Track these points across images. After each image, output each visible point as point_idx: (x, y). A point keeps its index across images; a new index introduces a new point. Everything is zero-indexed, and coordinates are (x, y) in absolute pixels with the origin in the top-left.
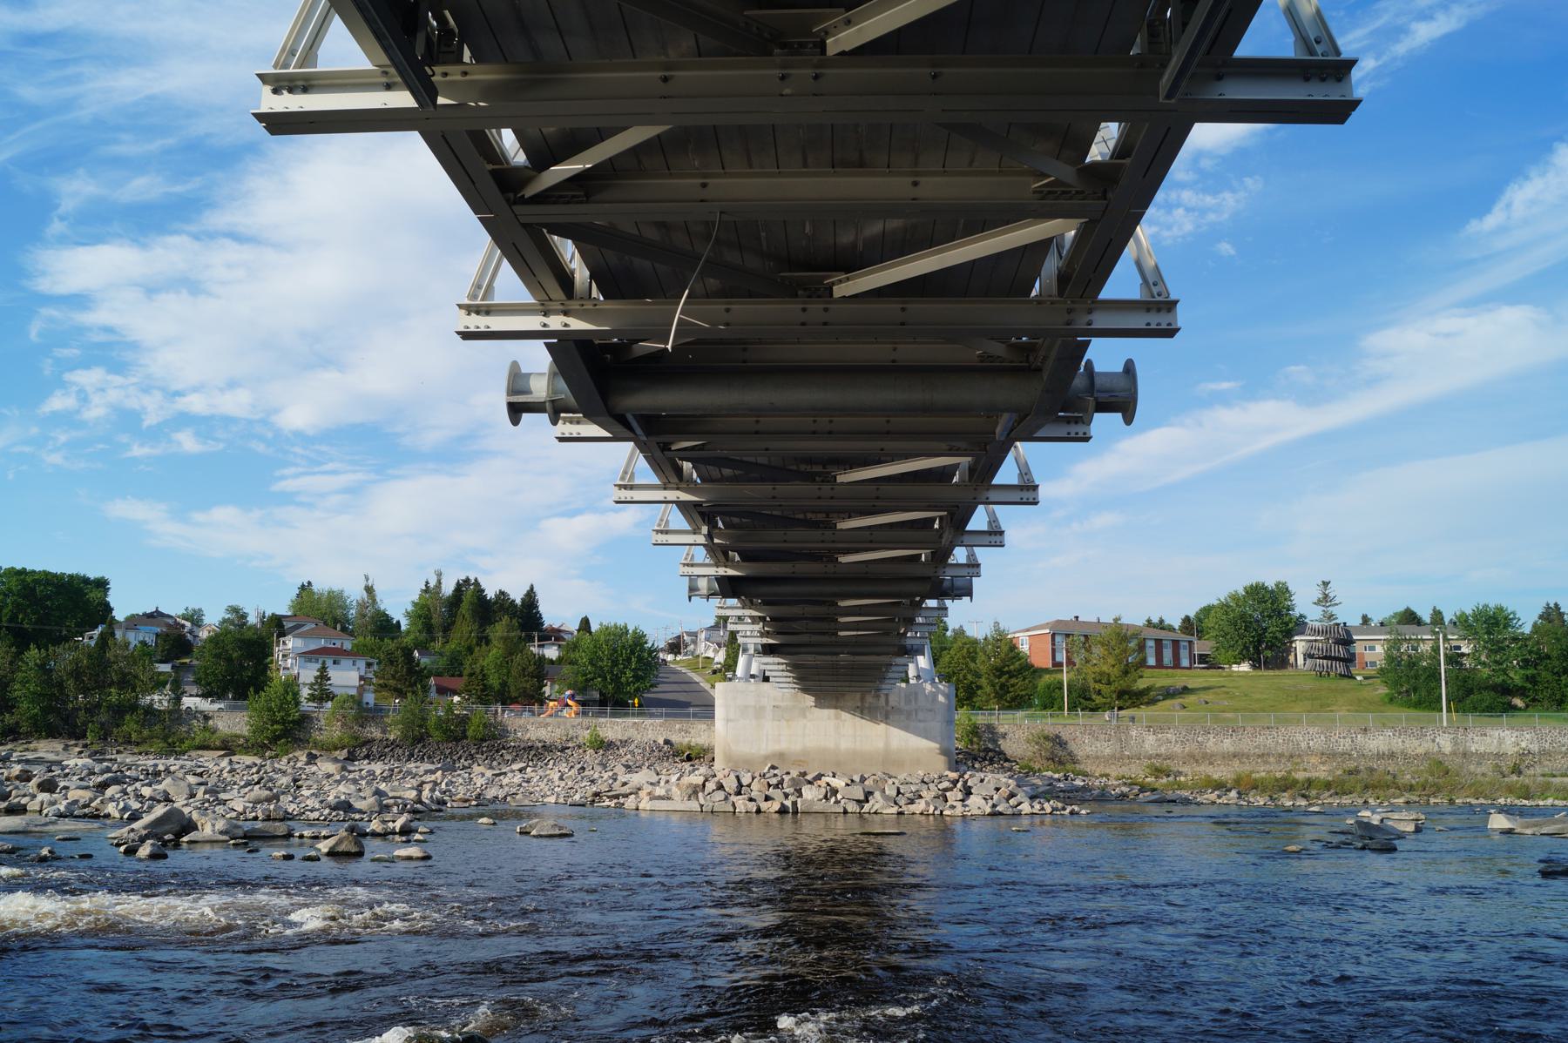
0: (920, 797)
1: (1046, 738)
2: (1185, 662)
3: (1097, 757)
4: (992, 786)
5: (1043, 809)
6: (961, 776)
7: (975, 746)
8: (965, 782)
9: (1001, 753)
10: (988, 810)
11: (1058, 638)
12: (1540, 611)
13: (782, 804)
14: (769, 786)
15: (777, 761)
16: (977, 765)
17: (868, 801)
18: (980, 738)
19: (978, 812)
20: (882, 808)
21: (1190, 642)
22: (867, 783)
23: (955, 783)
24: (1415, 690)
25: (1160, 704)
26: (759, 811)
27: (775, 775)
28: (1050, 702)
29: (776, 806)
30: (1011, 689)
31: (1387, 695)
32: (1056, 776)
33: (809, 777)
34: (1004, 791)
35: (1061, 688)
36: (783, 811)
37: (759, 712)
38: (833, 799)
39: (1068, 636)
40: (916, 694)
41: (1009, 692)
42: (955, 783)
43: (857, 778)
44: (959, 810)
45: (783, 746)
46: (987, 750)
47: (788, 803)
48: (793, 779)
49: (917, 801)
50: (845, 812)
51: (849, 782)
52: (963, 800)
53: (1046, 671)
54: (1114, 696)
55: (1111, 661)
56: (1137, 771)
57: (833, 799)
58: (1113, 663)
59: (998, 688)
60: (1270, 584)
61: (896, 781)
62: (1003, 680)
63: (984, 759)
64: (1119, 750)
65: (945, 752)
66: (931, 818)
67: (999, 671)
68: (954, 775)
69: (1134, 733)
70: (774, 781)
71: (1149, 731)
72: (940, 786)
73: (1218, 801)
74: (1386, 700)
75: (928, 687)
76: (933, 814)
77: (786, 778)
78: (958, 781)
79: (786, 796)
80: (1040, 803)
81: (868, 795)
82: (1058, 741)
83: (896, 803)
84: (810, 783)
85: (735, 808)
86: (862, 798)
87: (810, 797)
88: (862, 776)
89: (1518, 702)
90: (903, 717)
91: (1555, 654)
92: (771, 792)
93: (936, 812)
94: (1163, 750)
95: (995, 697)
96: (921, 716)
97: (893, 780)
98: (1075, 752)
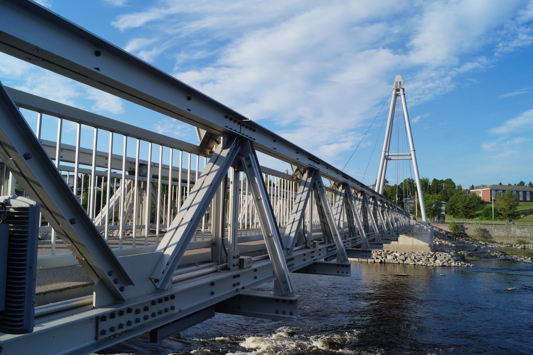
0: (421, 260)
1: (481, 230)
3: (499, 237)
4: (443, 257)
5: (458, 265)
6: (435, 254)
7: (457, 232)
8: (435, 256)
9: (466, 234)
10: (441, 265)
11: (493, 192)
13: (381, 260)
14: (378, 254)
16: (457, 238)
17: (406, 260)
18: (458, 229)
19: (438, 265)
20: (410, 262)
22: (406, 255)
23: (432, 256)
25: (528, 216)
26: (374, 262)
27: (380, 252)
28: (487, 215)
29: (379, 261)
30: (470, 213)
32: (483, 243)
33: (389, 252)
34: (447, 259)
35: (491, 210)
38: (396, 259)
39: (496, 191)
40: (422, 229)
41: (469, 214)
42: (432, 256)
43: (403, 253)
44: (432, 264)
46: (461, 233)
47: (383, 260)
48: (384, 253)
49: (420, 261)
50: (399, 263)
51: (401, 254)
52: (434, 261)
53: (488, 203)
54: (506, 216)
55: (506, 204)
56: (512, 241)
57: (396, 259)
58: (506, 205)
59: (465, 213)
61: (415, 255)
62: (467, 210)
63: (459, 236)
64: (507, 234)
65: (430, 246)
66: (424, 266)
67: (466, 207)
68: (432, 253)
69: (513, 229)
70: (379, 253)
71: (518, 228)
72: (428, 257)
73: (524, 261)
75: (425, 227)
76: (424, 265)
77: (383, 252)
78: (433, 255)
79: (382, 258)
80: (458, 263)
81: (406, 258)
82: (485, 231)
83: (414, 261)
84: (389, 254)
85: (368, 261)
86: (404, 259)
87: (389, 258)
88: (405, 253)
90: (418, 236)
92: (378, 257)
93: (425, 265)
94: (523, 235)
95: (464, 216)
96: (423, 235)
97: (414, 254)
98: (492, 235)
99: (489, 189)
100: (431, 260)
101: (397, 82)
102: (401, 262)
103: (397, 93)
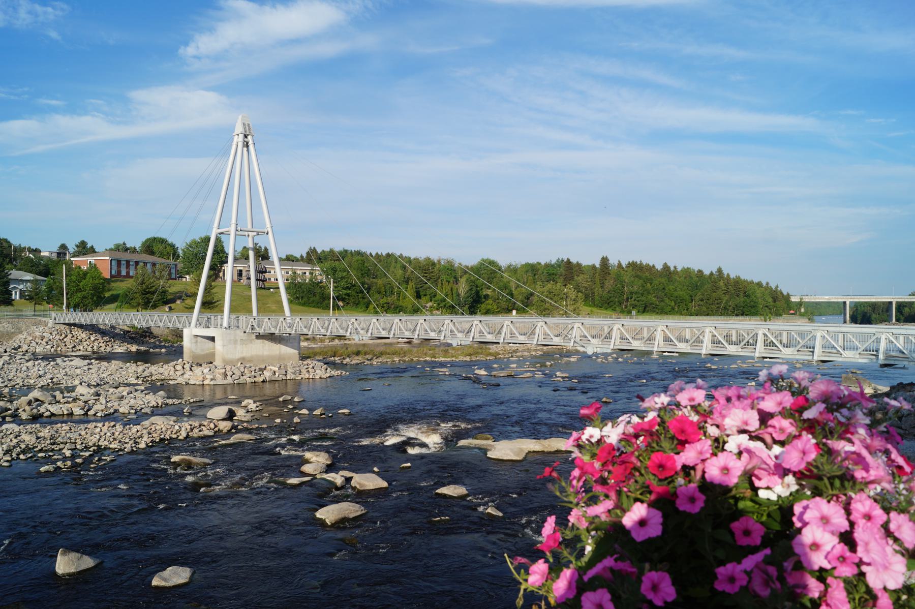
2: (173, 276)
9: (151, 333)
12: (307, 250)
15: (243, 360)
17: (286, 375)
21: (176, 265)
24: (302, 297)
36: (263, 381)
37: (235, 342)
70: (253, 369)
89: (341, 304)
99: (108, 258)
100: (304, 371)
101: (244, 124)
102: (284, 378)
103: (245, 139)
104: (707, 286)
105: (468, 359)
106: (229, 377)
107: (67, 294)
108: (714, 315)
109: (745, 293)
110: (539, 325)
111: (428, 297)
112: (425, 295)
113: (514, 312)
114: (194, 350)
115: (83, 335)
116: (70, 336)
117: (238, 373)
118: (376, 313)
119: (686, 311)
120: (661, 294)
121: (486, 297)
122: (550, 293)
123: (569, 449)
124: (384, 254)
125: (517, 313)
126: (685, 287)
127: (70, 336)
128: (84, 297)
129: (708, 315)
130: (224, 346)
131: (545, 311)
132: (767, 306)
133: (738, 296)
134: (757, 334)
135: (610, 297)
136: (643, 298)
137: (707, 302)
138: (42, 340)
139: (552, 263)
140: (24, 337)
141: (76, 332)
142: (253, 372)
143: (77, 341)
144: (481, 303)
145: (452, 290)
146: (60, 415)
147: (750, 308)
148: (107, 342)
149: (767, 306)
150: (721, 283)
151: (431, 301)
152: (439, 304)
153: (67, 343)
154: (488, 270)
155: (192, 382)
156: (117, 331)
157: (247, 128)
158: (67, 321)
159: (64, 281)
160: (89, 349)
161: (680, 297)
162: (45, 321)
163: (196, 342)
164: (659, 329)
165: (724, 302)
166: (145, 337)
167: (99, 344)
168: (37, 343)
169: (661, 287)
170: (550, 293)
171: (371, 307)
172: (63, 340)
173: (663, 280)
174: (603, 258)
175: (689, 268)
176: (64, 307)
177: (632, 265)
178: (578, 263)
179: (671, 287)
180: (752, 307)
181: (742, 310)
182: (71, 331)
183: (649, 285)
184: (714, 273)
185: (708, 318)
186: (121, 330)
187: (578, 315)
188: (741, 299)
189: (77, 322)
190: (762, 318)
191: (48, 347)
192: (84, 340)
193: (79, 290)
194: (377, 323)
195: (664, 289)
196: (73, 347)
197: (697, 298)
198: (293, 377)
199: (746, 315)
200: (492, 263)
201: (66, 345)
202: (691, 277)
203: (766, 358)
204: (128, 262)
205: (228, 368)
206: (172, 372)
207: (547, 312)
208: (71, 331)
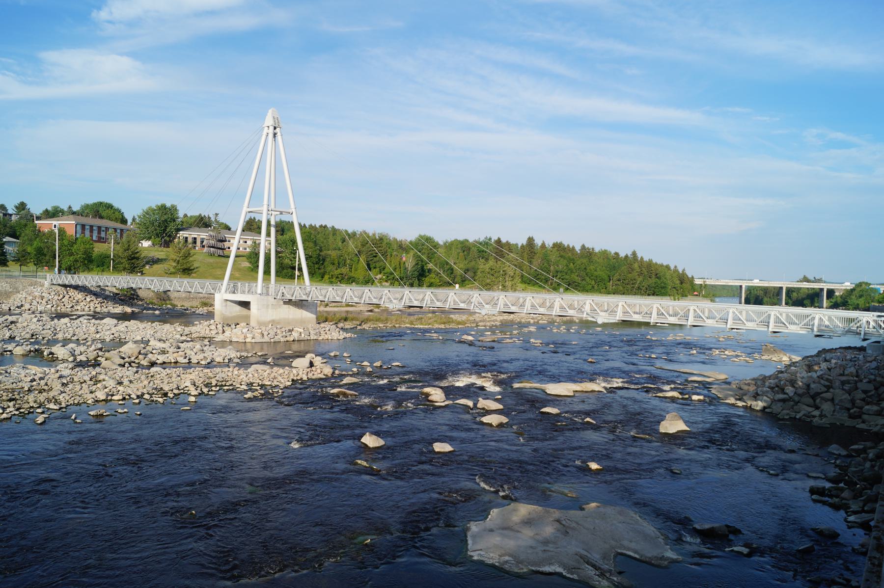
3: (179, 298)
9: (138, 296)
15: (273, 322)
31: (250, 267)
36: (293, 341)
45: (274, 318)
60: (168, 205)
74: (250, 270)
91: (315, 256)
99: (74, 222)
101: (274, 118)
104: (624, 268)
105: (443, 326)
106: (265, 336)
107: (59, 256)
108: (629, 294)
109: (656, 275)
110: (475, 296)
111: (378, 269)
112: (375, 268)
113: (457, 286)
114: (224, 312)
115: (79, 296)
116: (67, 297)
117: (272, 333)
118: (331, 283)
119: (604, 290)
120: (583, 273)
121: (430, 271)
122: (491, 269)
123: (601, 390)
124: (317, 226)
125: (459, 287)
126: (604, 268)
127: (67, 297)
128: (76, 261)
129: (624, 294)
130: (258, 309)
131: (488, 287)
132: (674, 288)
133: (650, 277)
134: (689, 310)
135: (538, 275)
136: (567, 277)
137: (623, 282)
138: (42, 300)
139: (481, 241)
140: (24, 296)
141: (72, 292)
142: (284, 333)
143: (74, 301)
144: (425, 277)
145: (400, 264)
146: (169, 363)
147: (660, 289)
148: (101, 303)
149: (674, 288)
150: (636, 266)
151: (380, 273)
152: (388, 277)
153: (65, 303)
154: (426, 245)
155: (234, 339)
156: (107, 293)
157: (276, 121)
158: (61, 283)
159: (57, 245)
160: (86, 309)
161: (600, 277)
162: (40, 282)
163: (226, 306)
164: (588, 303)
165: (638, 282)
166: (134, 299)
167: (94, 304)
168: (38, 303)
169: (583, 267)
170: (491, 269)
171: (326, 277)
172: (61, 300)
173: (584, 261)
174: (529, 238)
175: (605, 251)
176: (56, 269)
177: (558, 246)
178: (507, 242)
179: (592, 267)
180: (662, 288)
181: (653, 291)
182: (68, 292)
183: (572, 264)
184: (629, 255)
185: (624, 296)
186: (110, 292)
187: (515, 290)
188: (653, 280)
189: (73, 283)
190: (672, 298)
191: (49, 306)
192: (80, 301)
193: (71, 254)
194: (315, 290)
195: (585, 269)
196: (71, 307)
197: (615, 278)
198: (315, 337)
199: (657, 295)
200: (429, 239)
201: (64, 305)
202: (608, 258)
203: (734, 329)
204: (91, 227)
205: (263, 328)
206: (207, 332)
207: (489, 287)
208: (68, 292)
